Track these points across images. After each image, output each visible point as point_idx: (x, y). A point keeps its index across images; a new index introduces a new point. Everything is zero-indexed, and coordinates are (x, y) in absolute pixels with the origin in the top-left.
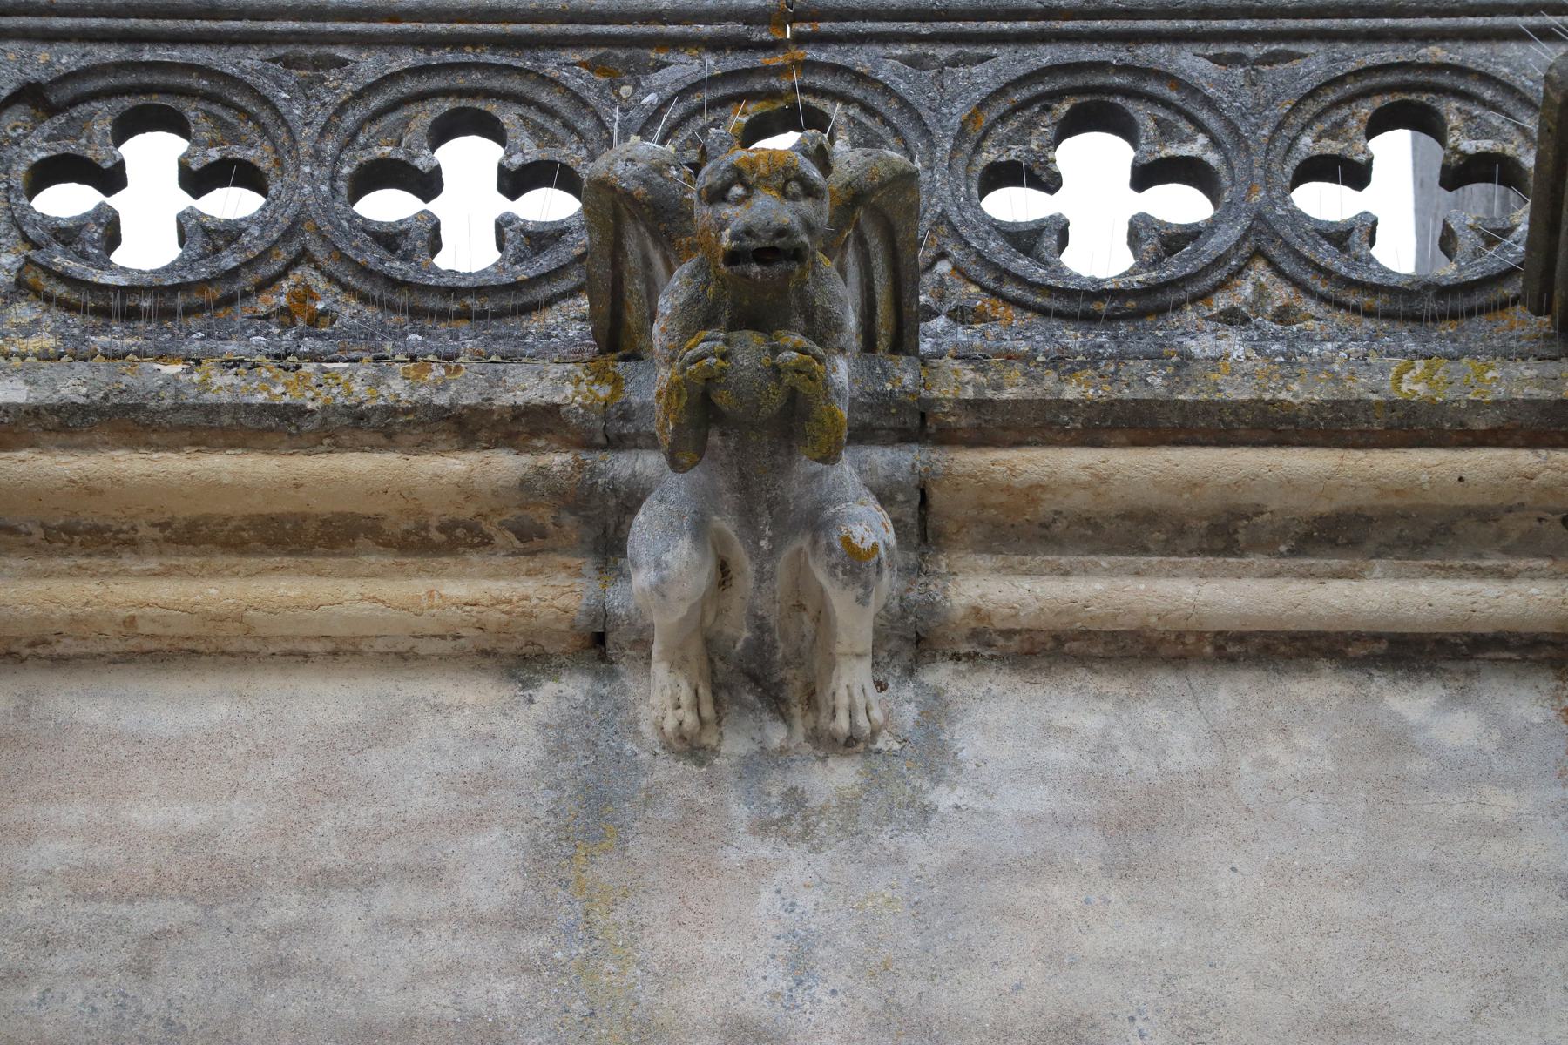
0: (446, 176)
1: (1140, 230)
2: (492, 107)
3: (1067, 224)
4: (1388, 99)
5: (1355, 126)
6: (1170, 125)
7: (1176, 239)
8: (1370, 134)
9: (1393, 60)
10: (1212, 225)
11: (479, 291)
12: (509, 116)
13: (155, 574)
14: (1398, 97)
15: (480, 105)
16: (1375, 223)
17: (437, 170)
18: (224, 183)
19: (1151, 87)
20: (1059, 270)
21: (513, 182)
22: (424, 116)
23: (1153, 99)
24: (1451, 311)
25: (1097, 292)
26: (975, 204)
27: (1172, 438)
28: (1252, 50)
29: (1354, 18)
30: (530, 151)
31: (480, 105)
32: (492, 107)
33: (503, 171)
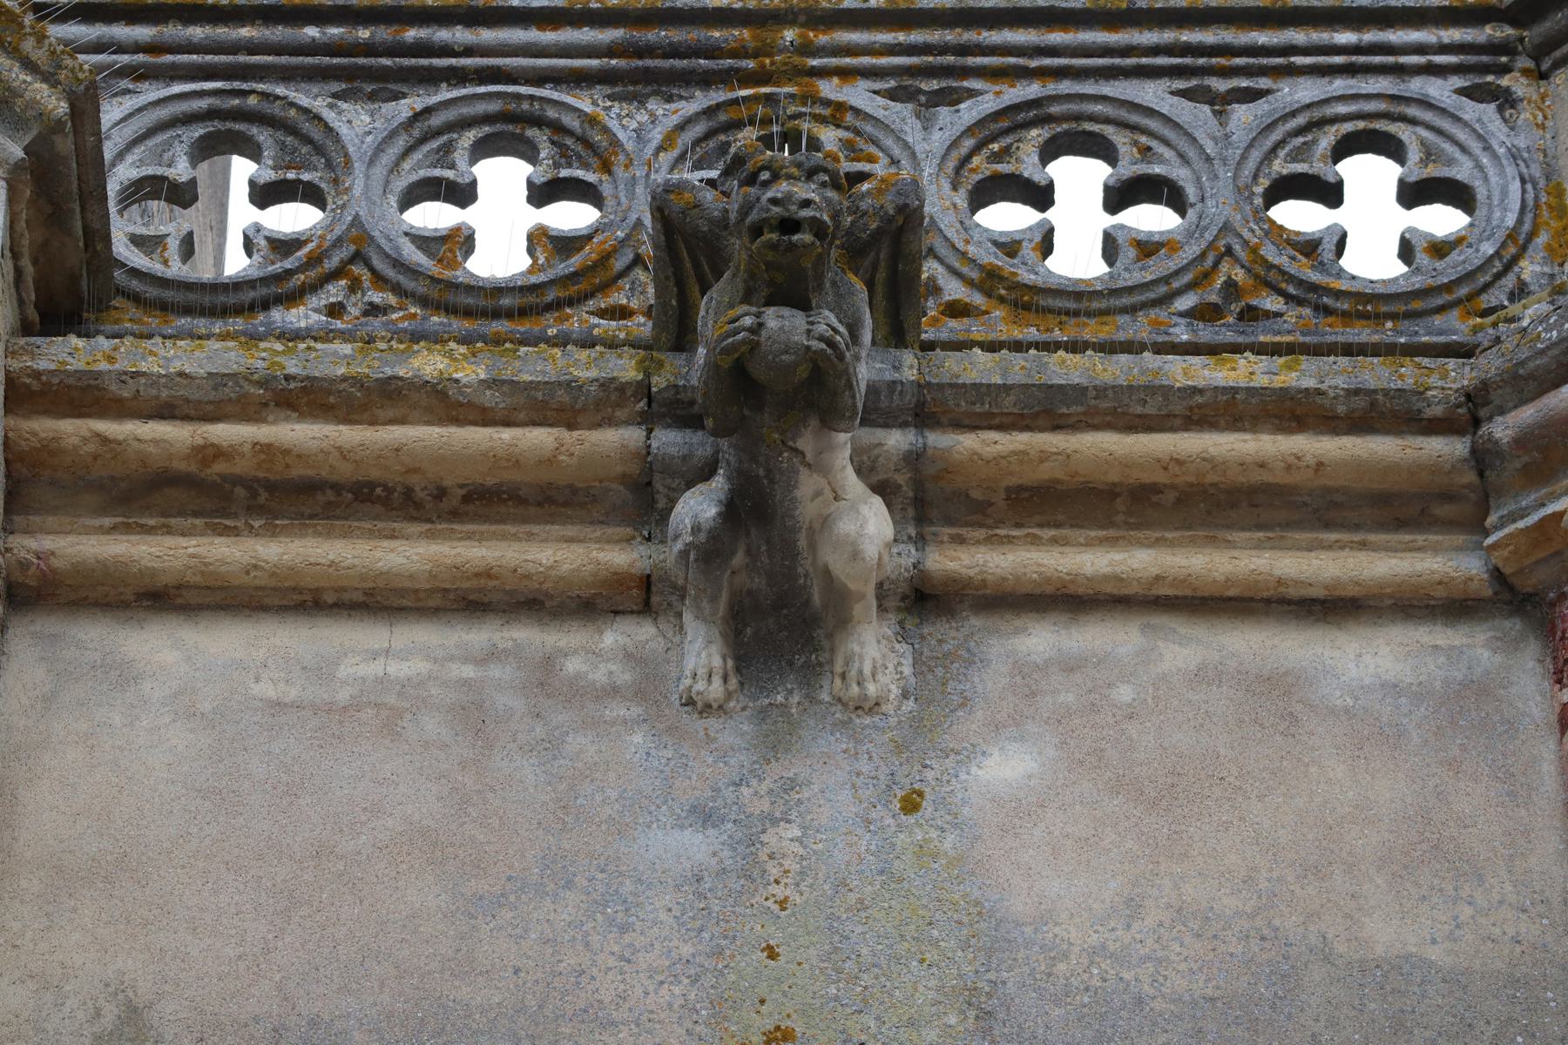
0: (481, 190)
1: (538, 238)
2: (1109, 131)
3: (474, 232)
4: (487, 129)
5: (460, 156)
6: (1149, 149)
7: (564, 244)
8: (473, 161)
9: (1111, 95)
10: (595, 231)
11: (1095, 295)
12: (1120, 139)
13: (114, 529)
14: (1361, 125)
15: (238, 127)
16: (1344, 236)
17: (474, 183)
18: (435, 197)
19: (1412, 111)
20: (1341, 273)
21: (541, 194)
22: (1326, 140)
23: (1413, 122)
24: (519, 309)
25: (497, 290)
26: (1260, 216)
27: (985, 424)
28: (1220, 85)
29: (1377, 55)
30: (1130, 167)
31: (238, 127)
32: (1109, 131)
33: (530, 184)
